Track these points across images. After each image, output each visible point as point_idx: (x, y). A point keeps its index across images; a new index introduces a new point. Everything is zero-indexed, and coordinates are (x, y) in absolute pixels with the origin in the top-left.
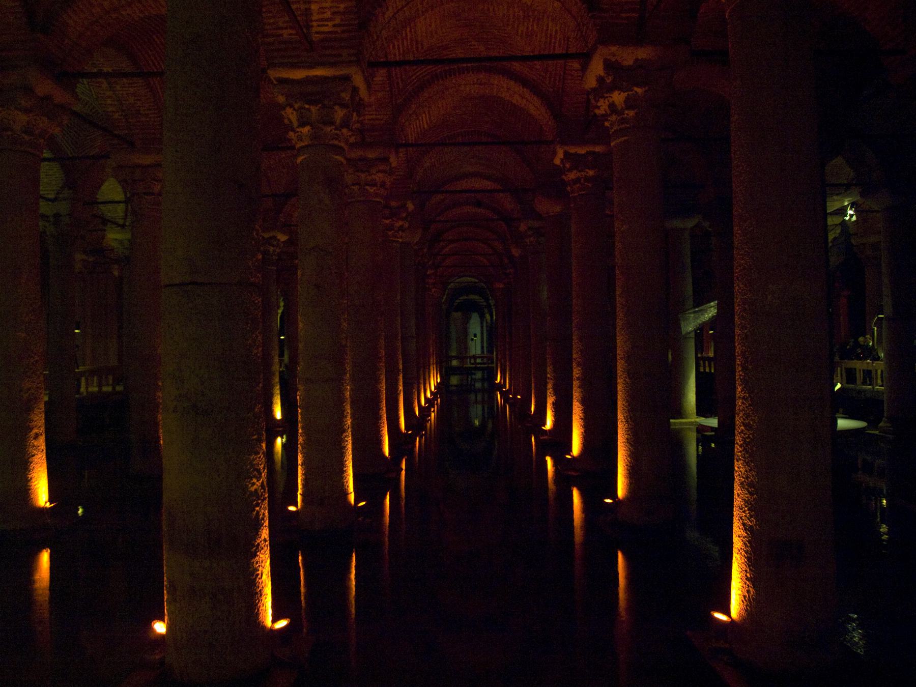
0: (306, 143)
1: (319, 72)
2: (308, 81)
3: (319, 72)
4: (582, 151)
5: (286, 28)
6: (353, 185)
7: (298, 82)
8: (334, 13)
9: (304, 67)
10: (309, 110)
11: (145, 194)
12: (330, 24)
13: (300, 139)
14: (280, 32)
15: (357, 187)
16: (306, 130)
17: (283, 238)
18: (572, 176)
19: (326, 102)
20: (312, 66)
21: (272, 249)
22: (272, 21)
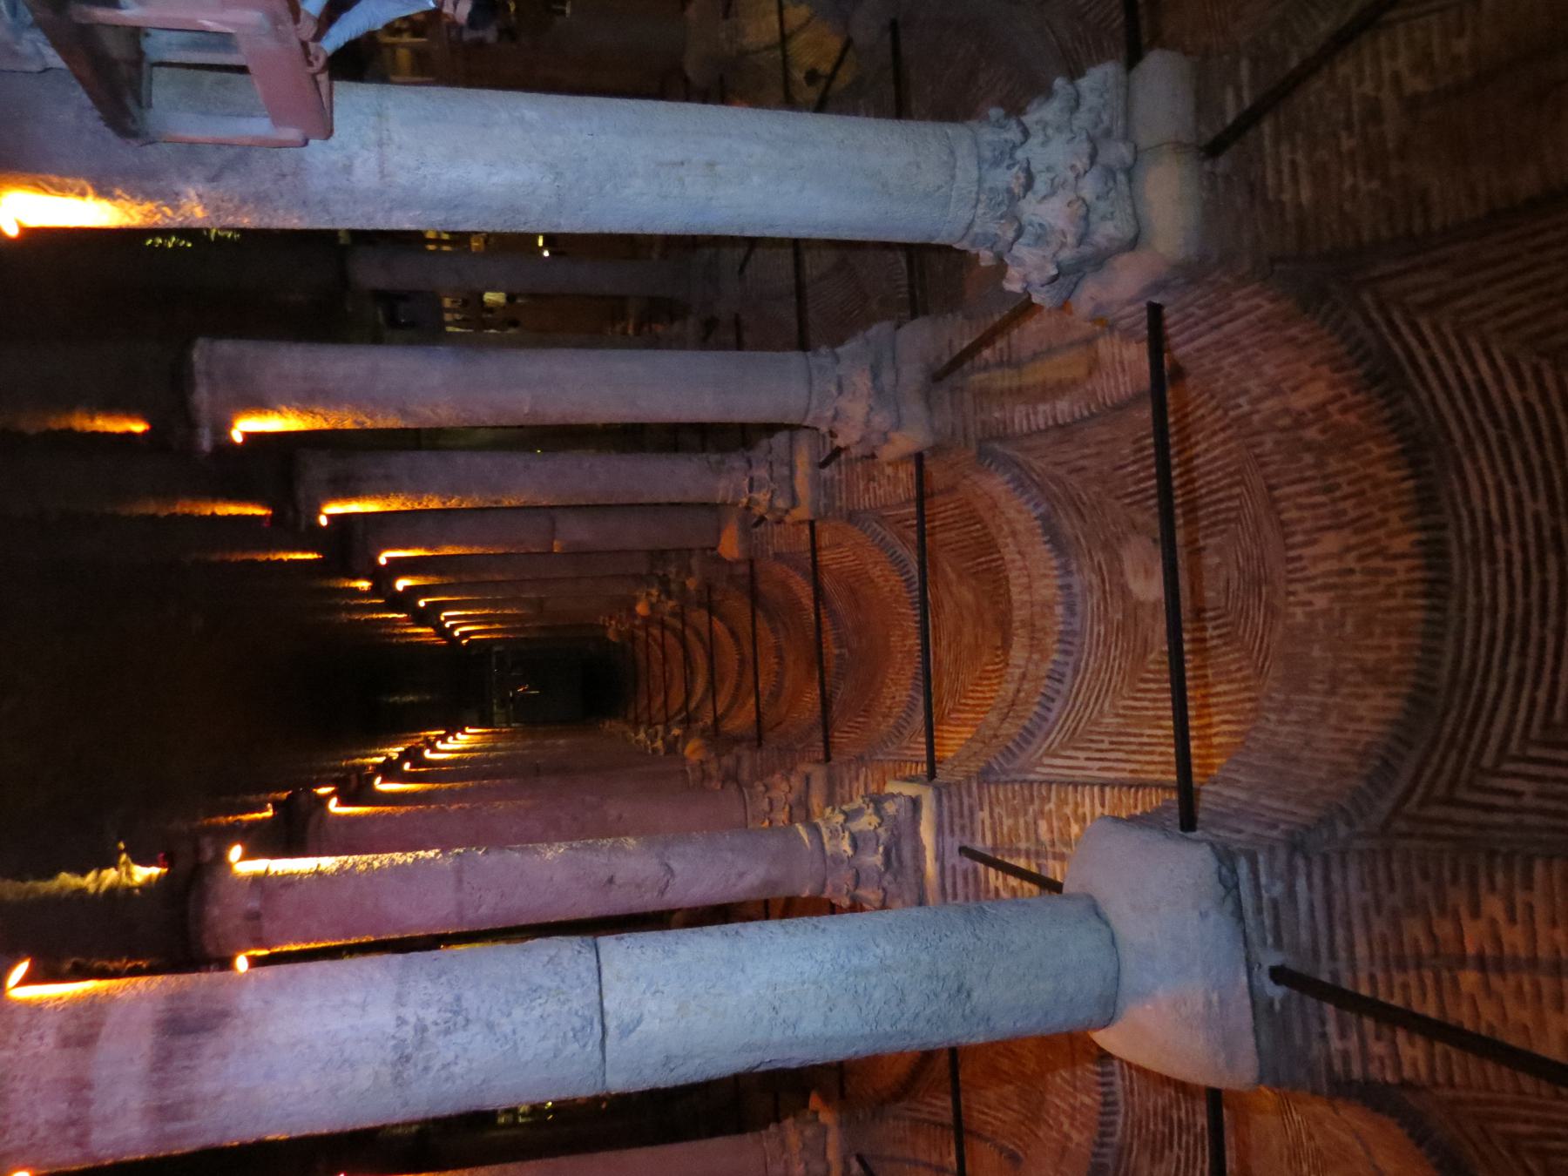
0: (827, 847)
1: (931, 867)
2: (918, 850)
3: (931, 867)
4: (832, 1155)
5: (992, 816)
6: (771, 803)
7: (916, 833)
8: (1014, 890)
9: (937, 842)
10: (876, 851)
11: (752, 479)
12: (1000, 883)
13: (834, 834)
14: (986, 808)
15: (767, 808)
16: (846, 846)
17: (692, 584)
18: (793, 1139)
19: (888, 877)
20: (940, 857)
21: (673, 570)
22: (1001, 797)
